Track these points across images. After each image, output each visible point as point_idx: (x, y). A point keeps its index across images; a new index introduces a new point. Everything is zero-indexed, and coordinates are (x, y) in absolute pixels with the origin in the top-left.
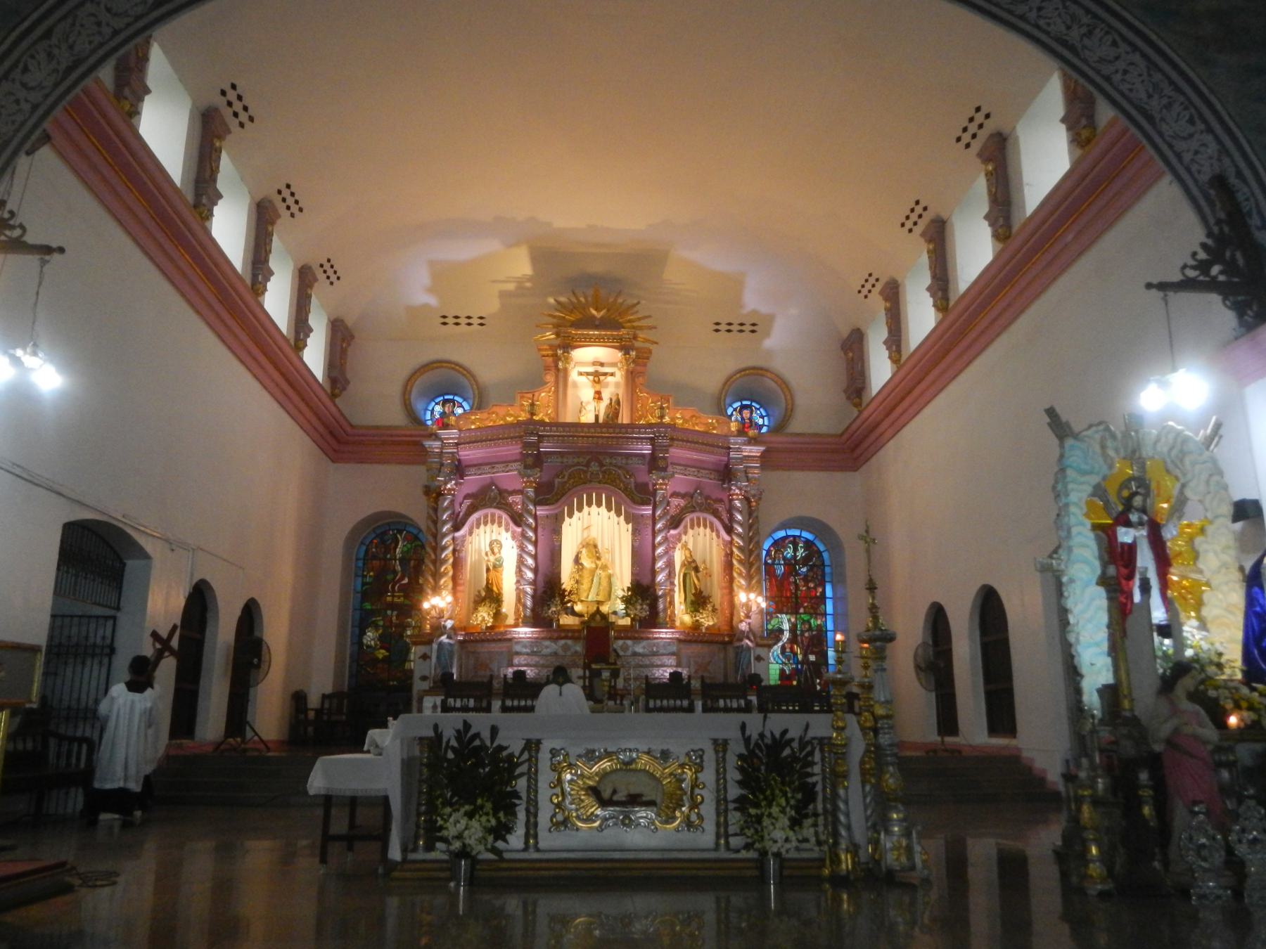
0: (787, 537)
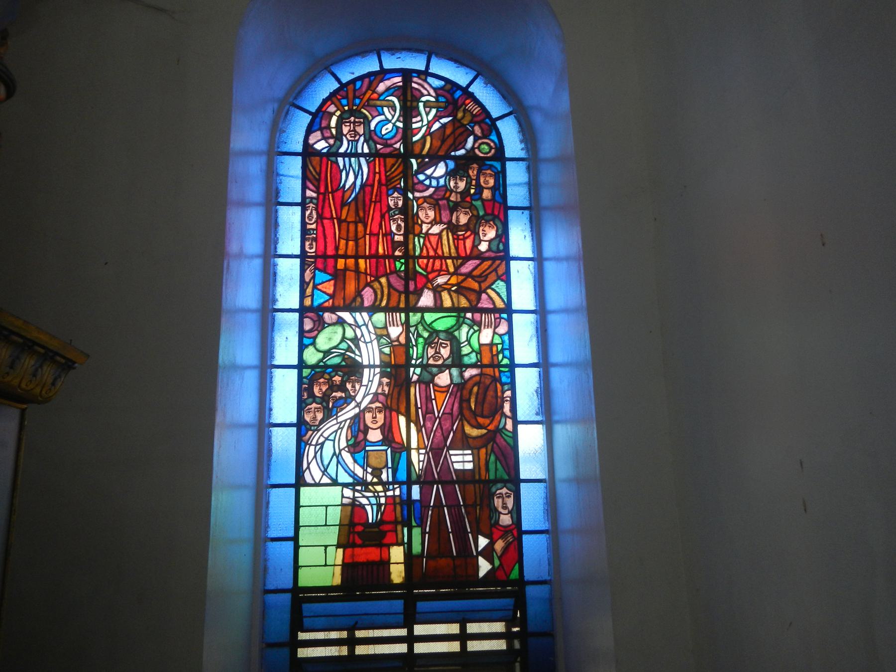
0: (383, 73)
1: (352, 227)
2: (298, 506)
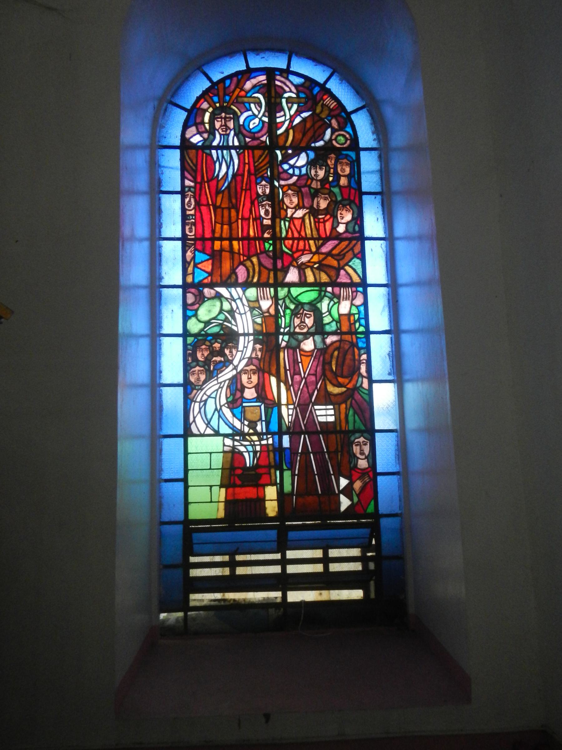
0: (249, 73)
1: (226, 213)
2: (186, 453)
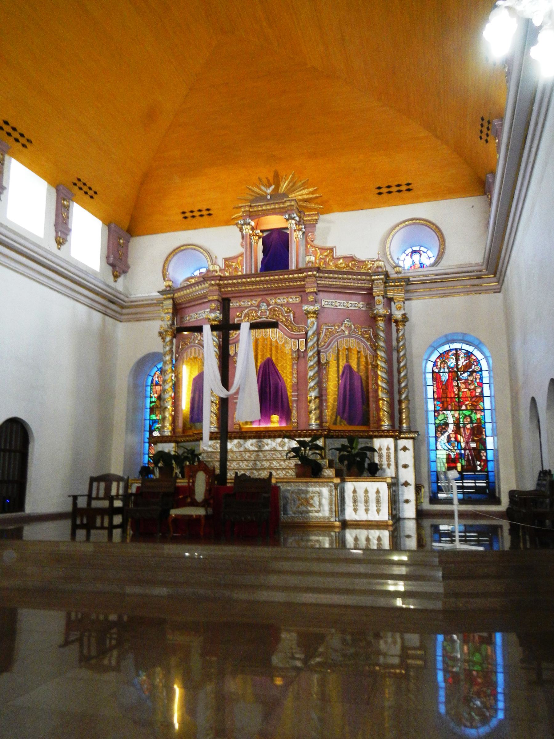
0: (450, 350)
2: (436, 454)
